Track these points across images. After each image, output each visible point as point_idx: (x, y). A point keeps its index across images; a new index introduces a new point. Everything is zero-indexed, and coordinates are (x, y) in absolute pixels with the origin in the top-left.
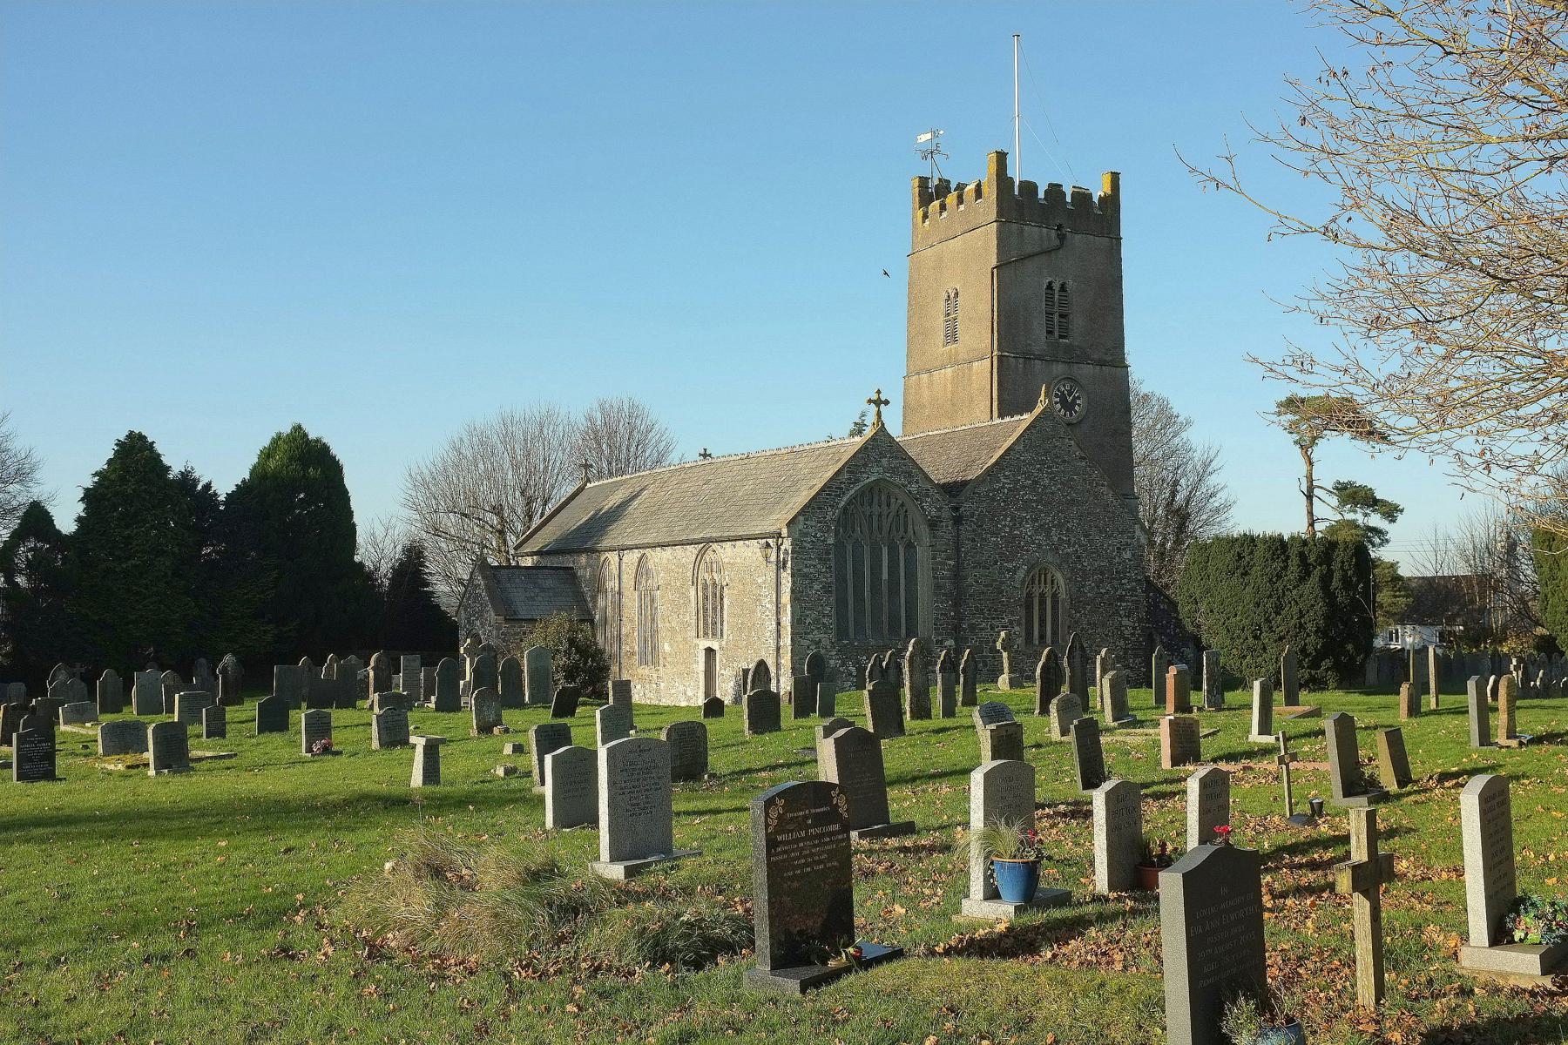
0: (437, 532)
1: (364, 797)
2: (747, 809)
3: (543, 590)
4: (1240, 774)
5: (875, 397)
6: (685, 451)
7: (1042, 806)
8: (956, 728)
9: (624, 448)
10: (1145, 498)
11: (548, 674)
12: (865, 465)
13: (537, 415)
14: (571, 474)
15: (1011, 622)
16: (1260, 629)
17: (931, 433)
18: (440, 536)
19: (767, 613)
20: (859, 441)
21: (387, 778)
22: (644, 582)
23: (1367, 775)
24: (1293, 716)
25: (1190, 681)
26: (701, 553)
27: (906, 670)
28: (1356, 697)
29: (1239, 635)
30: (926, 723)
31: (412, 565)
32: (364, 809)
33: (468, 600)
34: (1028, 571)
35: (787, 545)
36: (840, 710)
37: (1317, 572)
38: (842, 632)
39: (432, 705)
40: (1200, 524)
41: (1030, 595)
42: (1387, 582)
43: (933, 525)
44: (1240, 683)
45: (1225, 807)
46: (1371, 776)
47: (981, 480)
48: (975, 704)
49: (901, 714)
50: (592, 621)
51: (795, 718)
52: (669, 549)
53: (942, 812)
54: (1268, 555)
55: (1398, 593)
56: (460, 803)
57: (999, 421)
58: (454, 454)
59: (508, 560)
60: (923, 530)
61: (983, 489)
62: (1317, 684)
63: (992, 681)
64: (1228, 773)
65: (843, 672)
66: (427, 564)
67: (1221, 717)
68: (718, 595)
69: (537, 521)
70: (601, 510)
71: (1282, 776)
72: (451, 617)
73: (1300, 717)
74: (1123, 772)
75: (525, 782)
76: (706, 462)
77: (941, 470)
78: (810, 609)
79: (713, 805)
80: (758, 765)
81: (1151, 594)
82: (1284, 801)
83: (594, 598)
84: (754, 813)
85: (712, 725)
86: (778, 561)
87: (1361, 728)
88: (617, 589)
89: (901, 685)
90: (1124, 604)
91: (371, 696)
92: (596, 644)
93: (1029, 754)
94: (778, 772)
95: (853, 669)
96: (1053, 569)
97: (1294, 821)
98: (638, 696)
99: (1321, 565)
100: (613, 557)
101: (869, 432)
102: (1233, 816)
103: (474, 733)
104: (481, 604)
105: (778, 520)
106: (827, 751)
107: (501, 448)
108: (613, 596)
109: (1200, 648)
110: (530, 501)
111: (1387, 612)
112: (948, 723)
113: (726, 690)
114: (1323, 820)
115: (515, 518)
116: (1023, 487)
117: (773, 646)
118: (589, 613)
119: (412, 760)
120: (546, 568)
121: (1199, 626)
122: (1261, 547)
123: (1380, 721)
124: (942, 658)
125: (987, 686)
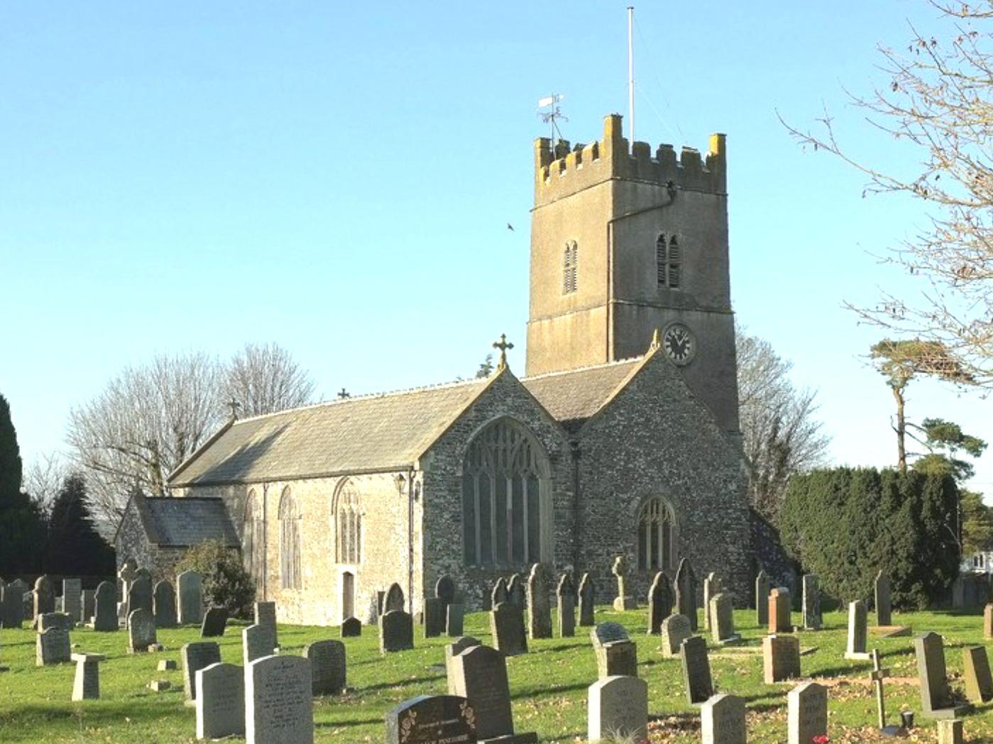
0: (96, 465)
1: (29, 710)
2: (382, 721)
3: (194, 519)
4: (837, 689)
5: (500, 341)
6: (323, 391)
7: (654, 718)
8: (574, 646)
9: (269, 388)
10: (750, 434)
11: (199, 596)
12: (491, 404)
13: (189, 358)
14: (220, 412)
15: (625, 549)
16: (855, 555)
17: (551, 374)
18: (99, 469)
19: (401, 540)
20: (485, 382)
21: (50, 691)
22: (287, 512)
23: (953, 690)
24: (885, 635)
25: (790, 604)
26: (340, 485)
27: (529, 593)
28: (944, 618)
29: (836, 562)
30: (547, 642)
31: (73, 494)
32: (29, 720)
33: (125, 528)
34: (642, 502)
35: (419, 477)
36: (468, 630)
37: (907, 503)
38: (470, 558)
39: (92, 625)
40: (800, 458)
41: (643, 524)
42: (972, 512)
43: (554, 459)
44: (835, 604)
45: (823, 719)
46: (958, 690)
47: (598, 417)
48: (591, 624)
49: (524, 633)
50: (239, 548)
51: (427, 637)
52: (310, 481)
53: (562, 724)
54: (863, 487)
55: (982, 522)
56: (117, 715)
57: (613, 363)
58: (111, 394)
59: (162, 491)
60: (545, 463)
61: (600, 426)
62: (907, 606)
63: (608, 603)
64: (826, 687)
65: (471, 595)
66: (87, 495)
67: (820, 636)
68: (356, 523)
69: (188, 455)
70: (247, 445)
71: (875, 690)
72: (109, 544)
73: (892, 636)
74: (729, 687)
75: (177, 697)
76: (344, 401)
77: (561, 408)
78: (440, 536)
79: (351, 716)
80: (392, 680)
81: (755, 523)
82: (877, 713)
83: (241, 527)
84: (388, 724)
85: (350, 644)
86: (411, 493)
87: (949, 646)
88: (262, 518)
89: (524, 606)
90: (730, 532)
91: (35, 617)
92: (243, 569)
93: (642, 670)
94: (411, 687)
95: (480, 592)
96: (664, 499)
97: (887, 732)
98: (281, 617)
99: (911, 495)
100: (258, 489)
101: (494, 374)
102: (830, 727)
103: (130, 650)
104: (137, 532)
105: (411, 455)
106: (456, 670)
107: (155, 388)
108: (258, 524)
109: (799, 572)
110: (181, 437)
111: (973, 539)
112: (568, 641)
113: (362, 612)
114: (913, 730)
115: (168, 453)
116: (637, 424)
117: (406, 571)
118: (236, 539)
119: (73, 676)
120: (196, 498)
121: (799, 552)
122: (856, 479)
123: (965, 640)
124: (562, 581)
125: (604, 607)
